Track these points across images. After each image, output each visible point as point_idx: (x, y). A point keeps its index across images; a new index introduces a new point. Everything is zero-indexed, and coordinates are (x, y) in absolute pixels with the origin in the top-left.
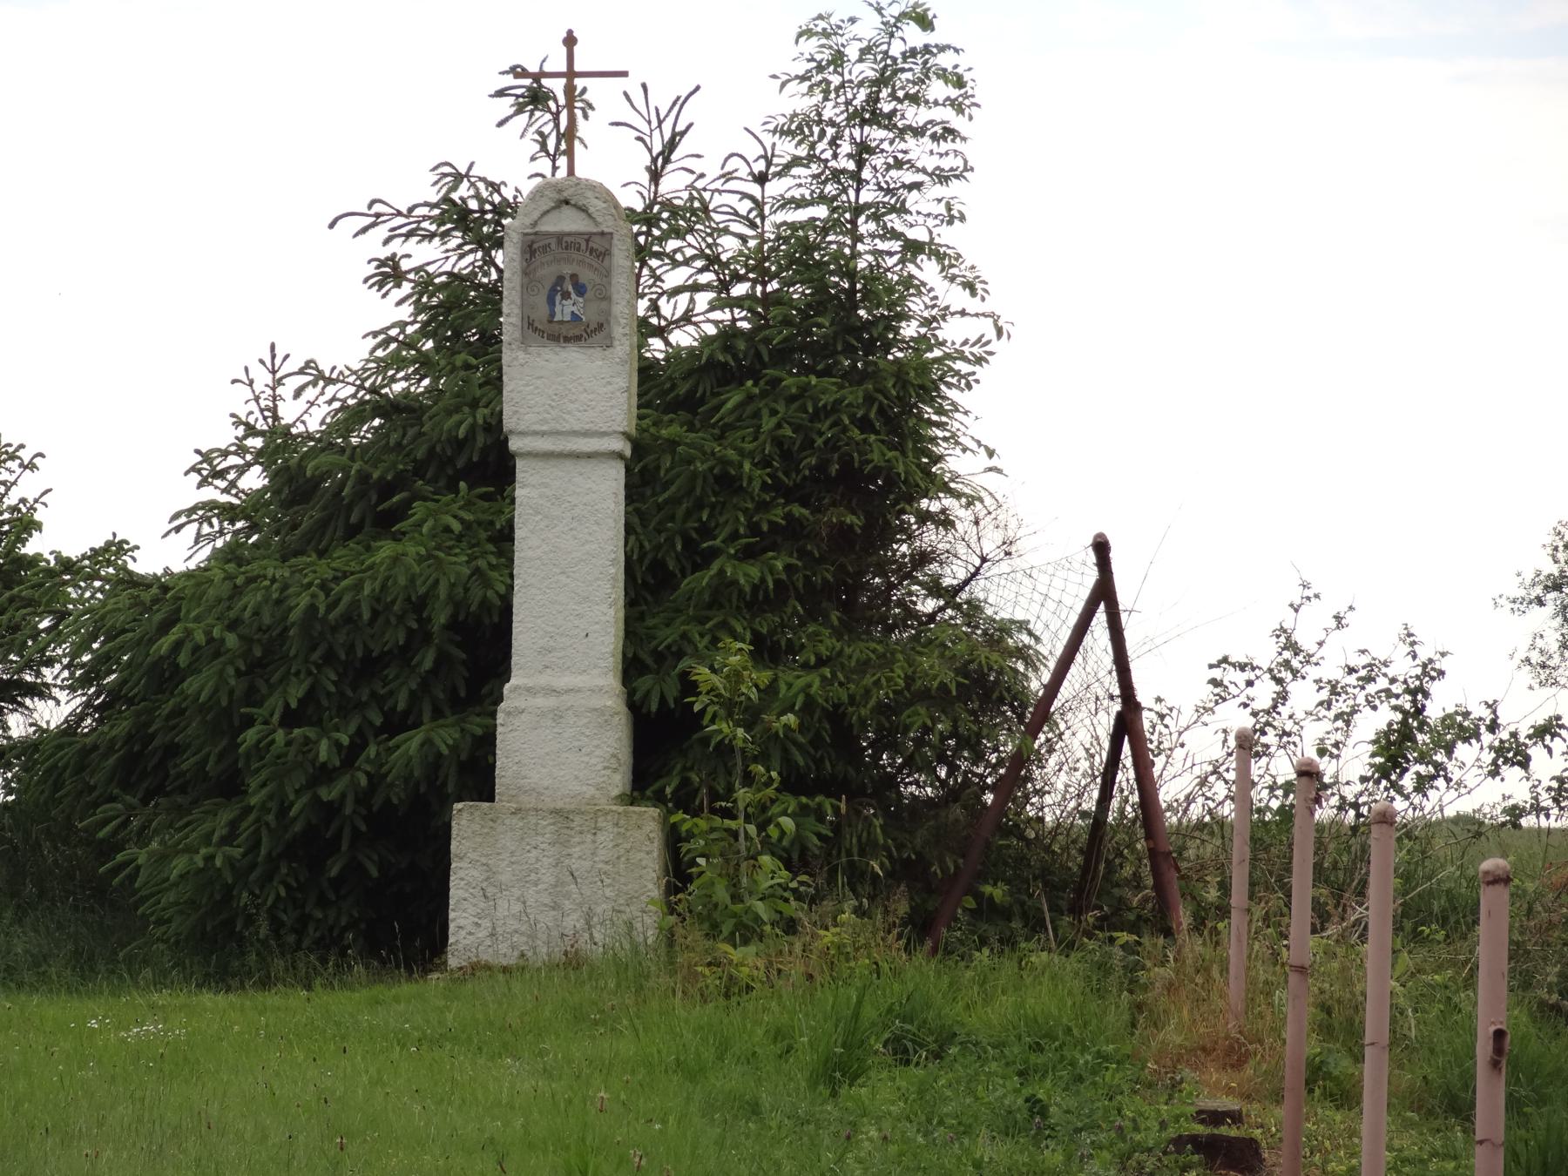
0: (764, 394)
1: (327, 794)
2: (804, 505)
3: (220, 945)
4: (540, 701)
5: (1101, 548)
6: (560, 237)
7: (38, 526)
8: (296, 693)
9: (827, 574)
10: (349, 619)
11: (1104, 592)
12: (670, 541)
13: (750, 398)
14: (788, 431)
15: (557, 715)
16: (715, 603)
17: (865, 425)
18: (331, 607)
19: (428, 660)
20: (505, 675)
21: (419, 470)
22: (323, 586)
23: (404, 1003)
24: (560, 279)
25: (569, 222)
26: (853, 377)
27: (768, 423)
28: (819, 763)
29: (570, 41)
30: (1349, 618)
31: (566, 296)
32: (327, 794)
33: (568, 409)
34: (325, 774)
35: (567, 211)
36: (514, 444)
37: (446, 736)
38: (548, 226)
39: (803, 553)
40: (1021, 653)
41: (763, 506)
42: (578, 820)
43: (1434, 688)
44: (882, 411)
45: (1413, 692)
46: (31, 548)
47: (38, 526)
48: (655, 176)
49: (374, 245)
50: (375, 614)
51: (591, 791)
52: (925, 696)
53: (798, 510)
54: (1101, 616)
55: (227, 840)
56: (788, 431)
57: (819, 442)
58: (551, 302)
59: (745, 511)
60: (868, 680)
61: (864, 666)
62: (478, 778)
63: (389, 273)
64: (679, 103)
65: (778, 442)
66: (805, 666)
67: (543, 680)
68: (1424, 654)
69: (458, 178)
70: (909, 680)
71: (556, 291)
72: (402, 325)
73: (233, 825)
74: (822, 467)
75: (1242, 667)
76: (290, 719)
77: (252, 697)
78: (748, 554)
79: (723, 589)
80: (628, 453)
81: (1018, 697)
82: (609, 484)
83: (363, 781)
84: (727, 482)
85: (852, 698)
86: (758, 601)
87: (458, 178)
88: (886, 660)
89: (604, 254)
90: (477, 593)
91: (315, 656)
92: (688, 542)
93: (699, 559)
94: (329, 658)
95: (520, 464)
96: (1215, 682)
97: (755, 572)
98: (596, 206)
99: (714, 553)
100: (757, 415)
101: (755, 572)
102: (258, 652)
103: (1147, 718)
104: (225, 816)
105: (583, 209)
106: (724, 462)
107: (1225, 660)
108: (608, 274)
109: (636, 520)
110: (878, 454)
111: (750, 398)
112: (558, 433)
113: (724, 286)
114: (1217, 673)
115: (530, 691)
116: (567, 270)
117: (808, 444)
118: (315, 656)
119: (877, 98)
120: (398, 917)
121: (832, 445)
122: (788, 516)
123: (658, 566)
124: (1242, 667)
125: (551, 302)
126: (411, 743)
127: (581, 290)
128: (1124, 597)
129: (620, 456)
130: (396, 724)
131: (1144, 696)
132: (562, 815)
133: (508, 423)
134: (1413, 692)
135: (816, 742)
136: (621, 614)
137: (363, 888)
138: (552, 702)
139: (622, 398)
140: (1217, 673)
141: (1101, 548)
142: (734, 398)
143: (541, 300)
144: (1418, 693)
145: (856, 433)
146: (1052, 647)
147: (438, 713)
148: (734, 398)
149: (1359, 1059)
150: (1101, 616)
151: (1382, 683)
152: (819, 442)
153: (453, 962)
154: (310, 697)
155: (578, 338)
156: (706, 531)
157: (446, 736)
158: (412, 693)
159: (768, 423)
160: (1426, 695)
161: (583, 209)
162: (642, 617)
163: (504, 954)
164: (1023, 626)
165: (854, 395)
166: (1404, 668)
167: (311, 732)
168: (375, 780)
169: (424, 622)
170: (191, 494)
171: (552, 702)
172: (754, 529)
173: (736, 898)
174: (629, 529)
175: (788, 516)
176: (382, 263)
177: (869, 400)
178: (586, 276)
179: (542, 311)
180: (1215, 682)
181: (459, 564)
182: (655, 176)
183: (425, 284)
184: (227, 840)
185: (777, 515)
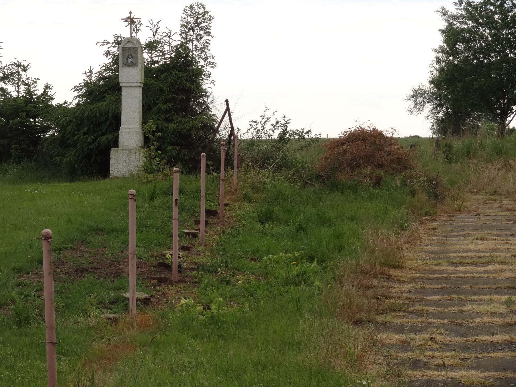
0: (169, 75)
1: (90, 147)
2: (176, 94)
3: (73, 174)
4: (126, 130)
5: (227, 101)
6: (128, 48)
7: (53, 99)
8: (86, 129)
9: (179, 107)
10: (96, 116)
11: (228, 110)
12: (151, 101)
13: (167, 76)
14: (173, 81)
15: (129, 133)
16: (159, 112)
17: (186, 80)
18: (91, 114)
19: (108, 123)
20: (121, 126)
21: (110, 89)
22: (91, 110)
23: (101, 184)
24: (129, 55)
25: (130, 45)
26: (185, 71)
27: (169, 80)
28: (177, 140)
29: (130, 13)
30: (276, 113)
31: (130, 58)
32: (90, 147)
33: (132, 79)
34: (90, 144)
35: (130, 43)
36: (121, 85)
37: (110, 136)
38: (126, 46)
39: (175, 103)
40: (214, 120)
41: (168, 95)
42: (132, 151)
43: (288, 125)
44: (190, 77)
45: (285, 126)
46: (54, 103)
47: (53, 99)
48: (154, 36)
50: (100, 115)
51: (135, 146)
52: (195, 128)
53: (174, 95)
54: (227, 113)
55: (74, 155)
56: (173, 81)
57: (179, 83)
58: (127, 59)
59: (165, 96)
60: (185, 125)
61: (185, 123)
62: (116, 144)
63: (108, 53)
64: (158, 22)
65: (171, 83)
66: (174, 123)
67: (127, 126)
68: (286, 120)
69: (118, 37)
70: (192, 125)
71: (128, 57)
72: (110, 63)
73: (76, 152)
74: (178, 88)
75: (255, 122)
76: (84, 134)
77: (79, 130)
78: (165, 103)
79: (159, 110)
80: (142, 85)
81: (212, 128)
82: (140, 91)
83: (97, 145)
84: (161, 90)
85: (182, 129)
86: (166, 112)
87: (118, 37)
88: (189, 122)
89: (137, 51)
90: (116, 111)
91: (89, 123)
92: (154, 101)
93: (156, 104)
94: (92, 123)
95: (122, 88)
96: (250, 125)
97: (165, 107)
98: (135, 42)
99: (158, 103)
100: (168, 79)
101: (165, 107)
102: (79, 122)
103: (235, 132)
104: (74, 151)
105: (133, 43)
106: (161, 87)
107: (252, 121)
108: (137, 54)
109: (145, 98)
110: (188, 85)
111: (167, 76)
112: (128, 83)
113: (164, 55)
114: (251, 123)
115: (124, 128)
116: (130, 54)
117: (176, 84)
118: (89, 123)
119: (197, 21)
120: (103, 169)
121: (181, 84)
122: (172, 97)
123: (149, 106)
124: (255, 122)
125: (127, 59)
126: (104, 138)
127: (132, 57)
128: (231, 110)
129: (140, 86)
130: (103, 134)
131: (235, 127)
132: (130, 150)
133: (120, 81)
134: (285, 126)
135: (176, 137)
136: (141, 114)
137: (96, 164)
138: (128, 130)
139: (140, 76)
140: (251, 123)
141: (227, 101)
142: (163, 76)
143: (125, 59)
144: (286, 126)
145: (185, 82)
146: (219, 119)
147: (110, 132)
148: (163, 76)
149: (199, 200)
150: (227, 113)
151: (279, 124)
152: (179, 83)
153: (111, 177)
154: (88, 130)
155: (132, 66)
156: (158, 99)
157: (110, 136)
158: (106, 129)
159: (169, 80)
160: (287, 126)
161: (133, 43)
162: (146, 115)
163: (120, 175)
164: (214, 115)
165: (185, 75)
166: (283, 122)
167: (87, 136)
168: (99, 144)
169: (108, 116)
170: (76, 93)
171: (128, 130)
172: (166, 99)
173: (151, 165)
174: (143, 99)
175: (172, 97)
176: (107, 51)
177: (187, 76)
178: (133, 55)
179: (126, 61)
180: (250, 125)
181: (113, 106)
182: (154, 36)
183: (114, 55)
184: (74, 155)
185: (170, 96)
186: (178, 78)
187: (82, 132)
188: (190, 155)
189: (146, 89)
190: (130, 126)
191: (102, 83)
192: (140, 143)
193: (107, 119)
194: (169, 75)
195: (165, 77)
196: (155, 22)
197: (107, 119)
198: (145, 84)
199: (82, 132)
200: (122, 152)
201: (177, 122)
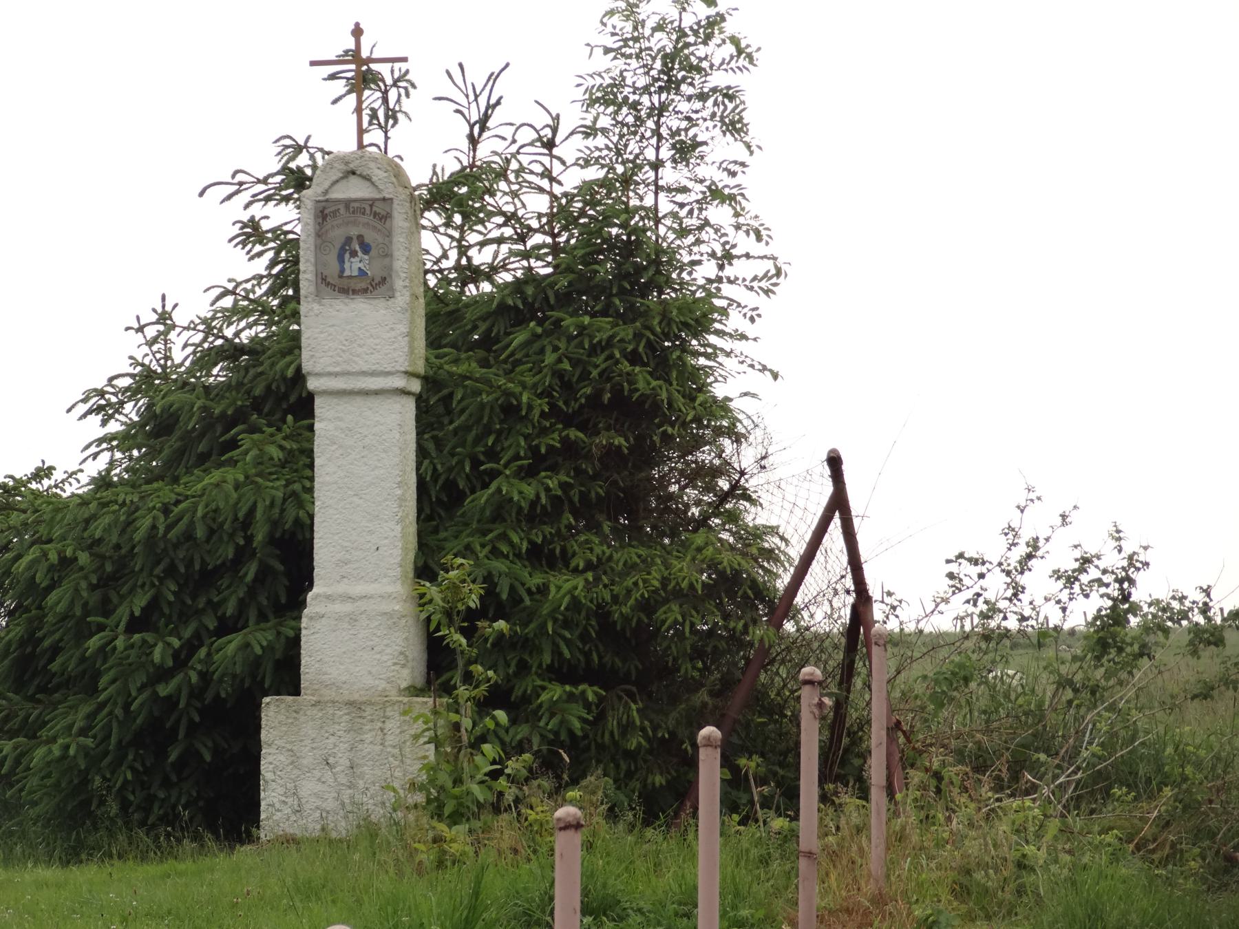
0: (547, 333)
1: (163, 690)
2: (581, 428)
4: (338, 607)
5: (835, 462)
6: (347, 203)
8: (139, 603)
9: (599, 489)
10: (189, 536)
11: (839, 503)
12: (461, 463)
13: (537, 337)
14: (566, 366)
15: (353, 619)
17: (634, 358)
18: (169, 528)
19: (251, 571)
20: (311, 586)
21: (257, 405)
22: (166, 510)
24: (349, 240)
25: (355, 190)
27: (550, 358)
28: (588, 655)
29: (357, 32)
30: (1074, 517)
31: (354, 254)
32: (163, 690)
33: (364, 354)
34: (163, 674)
35: (353, 180)
36: (312, 384)
37: (260, 637)
38: (337, 194)
39: (579, 472)
40: (770, 554)
41: (544, 431)
42: (369, 710)
43: (1139, 577)
44: (650, 346)
45: (1120, 581)
48: (473, 141)
49: (237, 211)
50: (211, 532)
52: (678, 594)
53: (574, 434)
54: (837, 521)
55: (83, 732)
56: (566, 366)
57: (595, 373)
58: (341, 260)
59: (526, 437)
60: (629, 582)
61: (630, 568)
62: (285, 673)
63: (252, 233)
64: (493, 78)
65: (559, 375)
66: (576, 571)
67: (341, 588)
69: (299, 149)
70: (665, 581)
71: (345, 250)
73: (91, 716)
75: (975, 562)
76: (135, 625)
77: (106, 608)
78: (528, 473)
80: (416, 386)
81: (760, 592)
83: (194, 678)
84: (510, 410)
85: (615, 598)
86: (533, 515)
87: (299, 149)
88: (647, 563)
89: (386, 217)
91: (158, 570)
92: (476, 463)
93: (485, 479)
94: (171, 571)
95: (318, 402)
96: (951, 576)
97: (529, 490)
98: (378, 175)
99: (493, 475)
100: (542, 351)
101: (529, 490)
102: (109, 568)
103: (878, 612)
104: (85, 709)
105: (367, 178)
106: (507, 394)
107: (961, 556)
108: (389, 234)
109: (431, 446)
110: (644, 381)
112: (348, 373)
113: (522, 238)
114: (953, 568)
115: (328, 597)
116: (354, 232)
117: (585, 376)
118: (158, 570)
121: (605, 375)
122: (565, 441)
123: (450, 486)
124: (975, 562)
125: (341, 260)
126: (232, 644)
127: (366, 249)
128: (856, 503)
129: (404, 392)
130: (226, 627)
131: (874, 591)
133: (306, 367)
135: (584, 637)
136: (413, 529)
138: (348, 607)
140: (953, 568)
141: (835, 462)
142: (520, 338)
144: (1125, 580)
145: (626, 366)
146: (796, 551)
147: (262, 617)
148: (520, 338)
150: (837, 521)
151: (1094, 573)
152: (595, 373)
155: (365, 291)
156: (492, 455)
157: (260, 637)
158: (241, 602)
159: (550, 358)
160: (1132, 582)
161: (367, 178)
162: (436, 531)
163: (310, 825)
164: (774, 530)
165: (626, 332)
167: (149, 637)
168: (205, 676)
169: (249, 539)
170: (94, 428)
171: (348, 607)
172: (534, 451)
173: (458, 781)
174: (422, 453)
175: (565, 441)
176: (245, 225)
177: (638, 336)
178: (370, 236)
180: (951, 576)
181: (275, 489)
182: (473, 141)
184: (83, 732)
185: (554, 440)
186: (594, 350)
187: (122, 614)
188: (655, 730)
189: (435, 406)
190: (358, 589)
191: (218, 374)
192: (406, 672)
193: (243, 554)
194: (547, 333)
195: (527, 343)
196: (477, 77)
197: (243, 554)
198: (431, 382)
199: (122, 614)
200: (314, 712)
201: (589, 566)
